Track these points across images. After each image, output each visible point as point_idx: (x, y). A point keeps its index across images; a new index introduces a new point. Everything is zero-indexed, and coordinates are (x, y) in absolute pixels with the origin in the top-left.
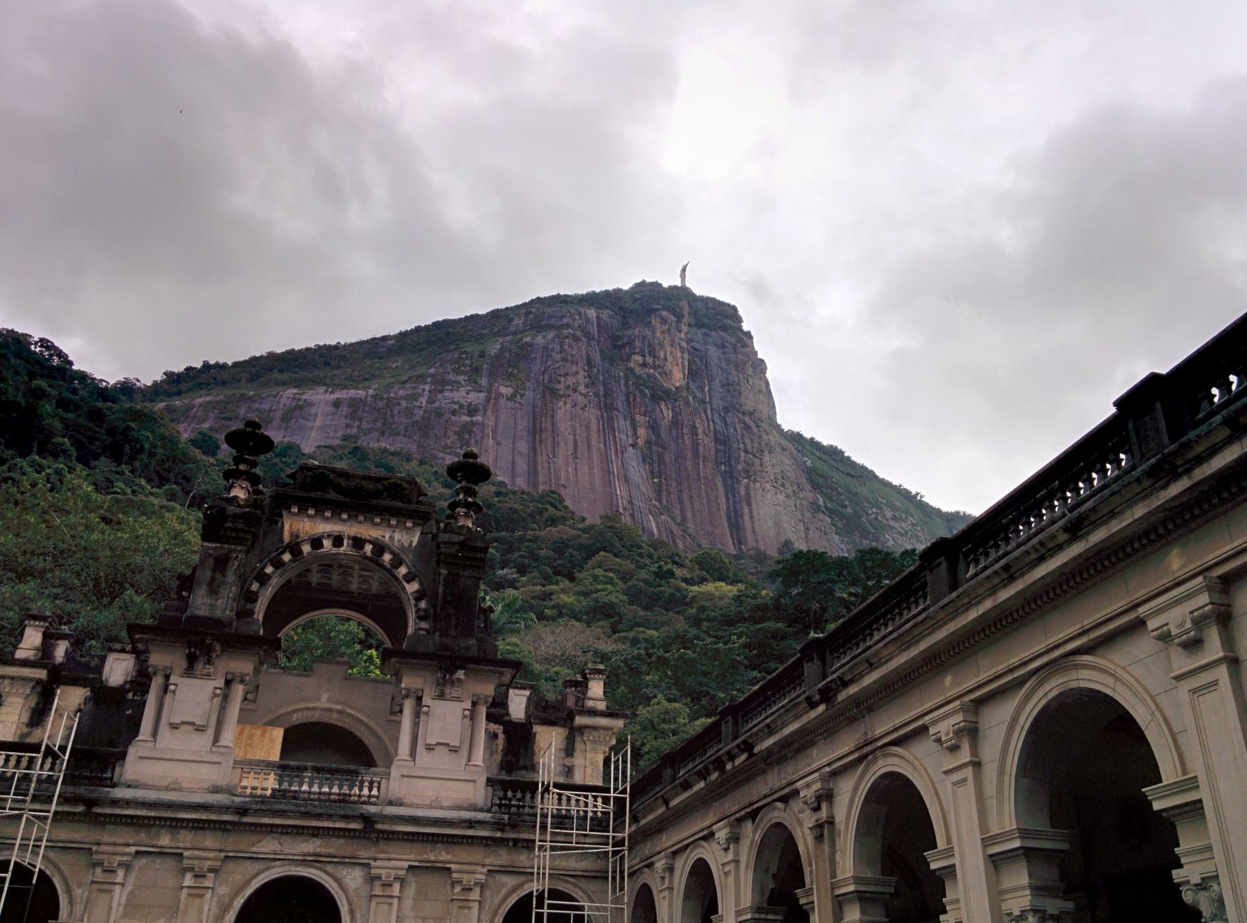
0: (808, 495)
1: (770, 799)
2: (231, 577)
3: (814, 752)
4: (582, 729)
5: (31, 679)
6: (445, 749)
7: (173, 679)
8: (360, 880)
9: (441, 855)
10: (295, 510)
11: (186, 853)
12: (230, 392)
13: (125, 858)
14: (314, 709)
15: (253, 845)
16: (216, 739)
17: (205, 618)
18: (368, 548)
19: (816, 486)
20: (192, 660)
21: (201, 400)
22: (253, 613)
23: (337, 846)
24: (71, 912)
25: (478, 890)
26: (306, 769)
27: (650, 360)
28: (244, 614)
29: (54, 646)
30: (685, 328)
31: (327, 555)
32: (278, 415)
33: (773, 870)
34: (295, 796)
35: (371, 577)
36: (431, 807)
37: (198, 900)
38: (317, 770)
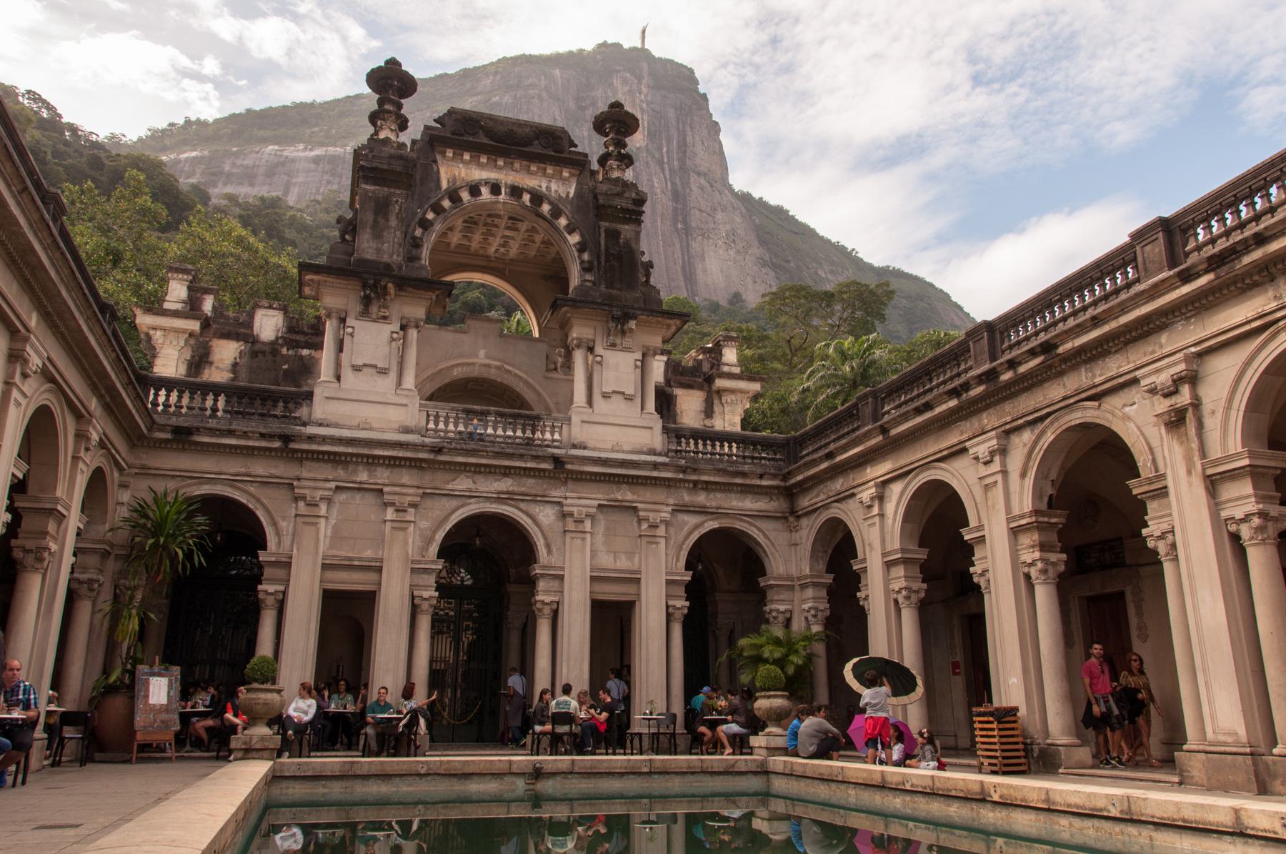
0: (756, 250)
1: (1072, 401)
2: (393, 222)
3: (1164, 338)
4: (720, 392)
5: (184, 331)
6: (620, 397)
7: (350, 322)
8: (553, 518)
9: (625, 494)
10: (450, 153)
11: (386, 489)
13: (326, 493)
14: (473, 364)
15: (448, 483)
16: (399, 383)
17: (373, 261)
18: (526, 198)
19: (763, 243)
20: (367, 302)
21: (185, 155)
22: (420, 259)
23: (530, 485)
24: (279, 544)
25: (663, 528)
26: (487, 413)
28: (412, 259)
29: (201, 301)
30: (644, 90)
31: (484, 204)
32: (262, 170)
33: (1054, 475)
34: (481, 438)
35: (513, 238)
36: (613, 451)
37: (401, 534)
38: (502, 415)
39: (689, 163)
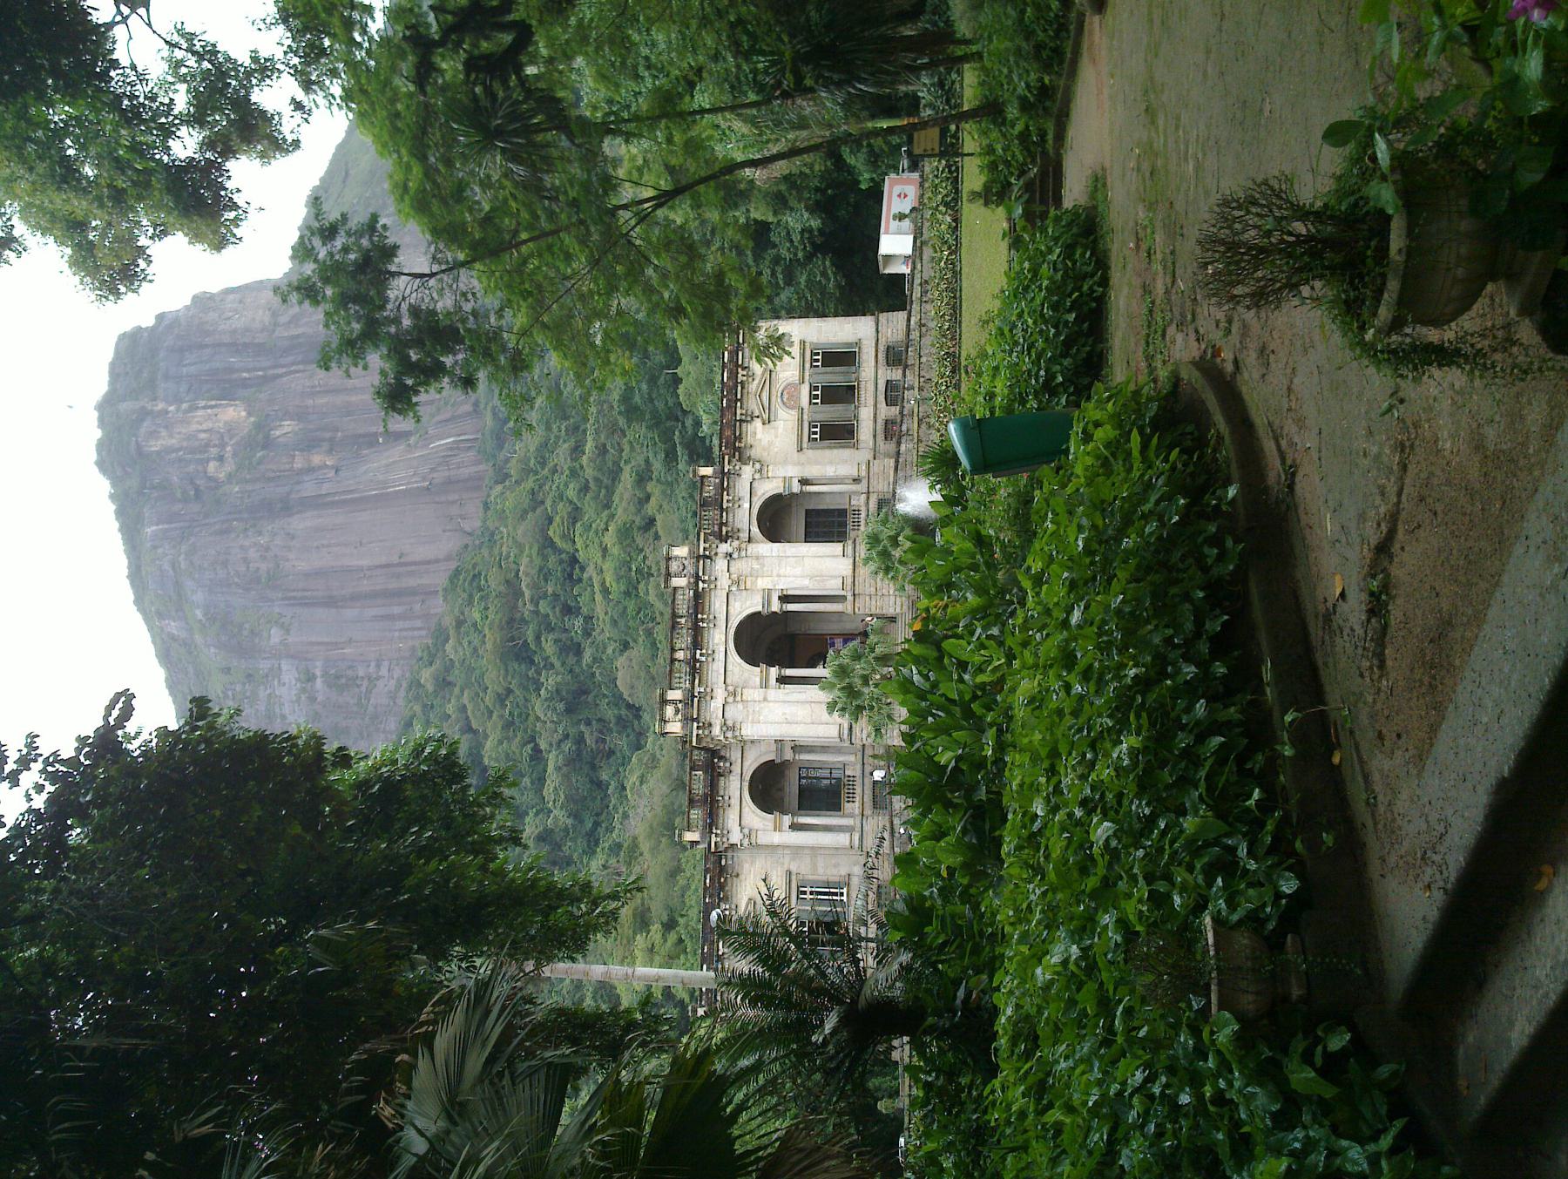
27: (214, 451)
39: (260, 338)
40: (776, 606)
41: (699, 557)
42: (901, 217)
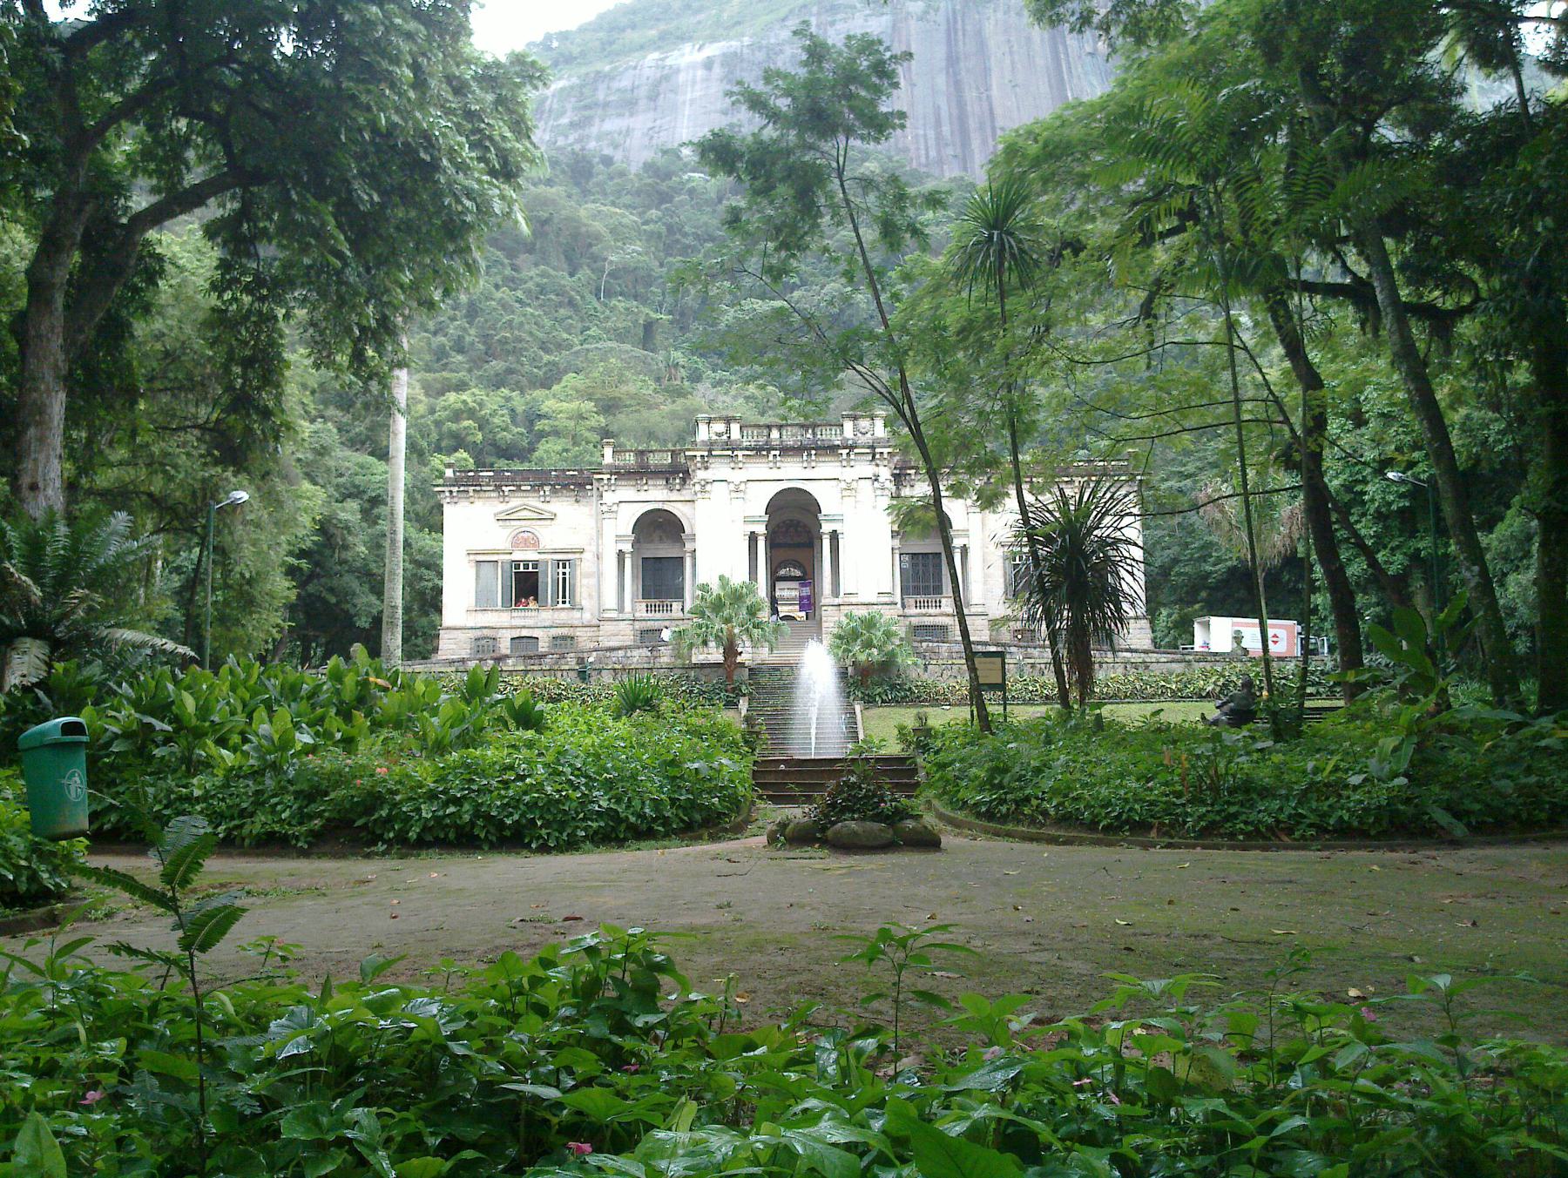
12: (583, 70)
32: (643, 92)
40: (826, 528)
41: (873, 447)
42: (1238, 638)
